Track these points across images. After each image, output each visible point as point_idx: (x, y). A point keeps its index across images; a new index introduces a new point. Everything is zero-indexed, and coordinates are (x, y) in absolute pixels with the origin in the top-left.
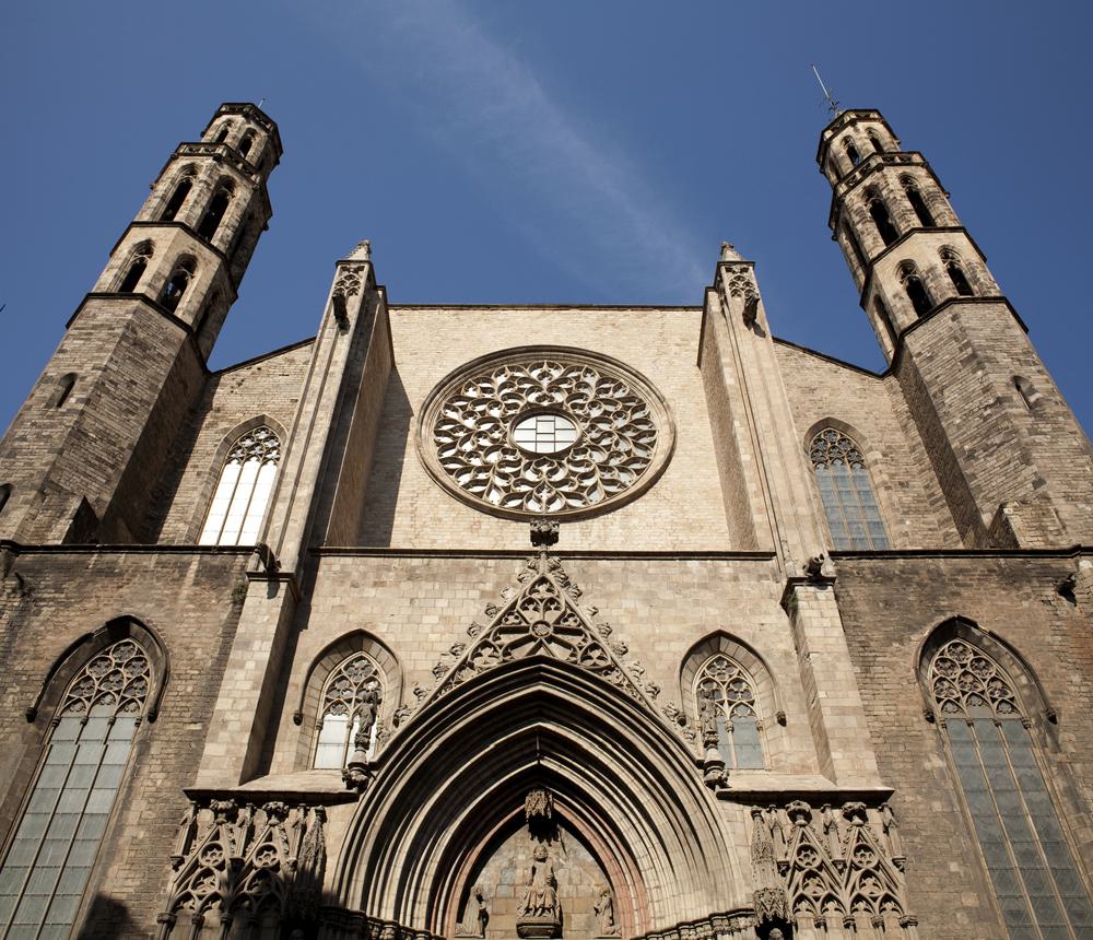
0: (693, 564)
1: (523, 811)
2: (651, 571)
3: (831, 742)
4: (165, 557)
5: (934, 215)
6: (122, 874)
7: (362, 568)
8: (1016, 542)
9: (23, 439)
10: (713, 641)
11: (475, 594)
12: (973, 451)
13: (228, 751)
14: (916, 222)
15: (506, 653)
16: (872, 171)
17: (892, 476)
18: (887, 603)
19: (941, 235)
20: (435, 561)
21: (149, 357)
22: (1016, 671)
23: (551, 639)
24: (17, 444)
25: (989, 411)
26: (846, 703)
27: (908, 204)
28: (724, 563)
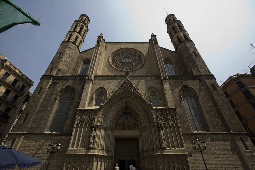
0: (148, 77)
1: (125, 112)
2: (142, 78)
3: (168, 102)
4: (74, 77)
5: (182, 29)
6: (69, 120)
7: (102, 78)
8: (194, 75)
9: (54, 61)
10: (151, 88)
11: (117, 82)
12: (187, 62)
13: (83, 103)
14: (179, 30)
15: (122, 90)
16: (173, 23)
17: (176, 65)
18: (176, 83)
19: (183, 32)
20: (112, 77)
21: (71, 50)
22: (193, 92)
23: (128, 88)
24: (53, 62)
25: (190, 56)
26: (170, 96)
27: (178, 28)
28: (152, 77)
